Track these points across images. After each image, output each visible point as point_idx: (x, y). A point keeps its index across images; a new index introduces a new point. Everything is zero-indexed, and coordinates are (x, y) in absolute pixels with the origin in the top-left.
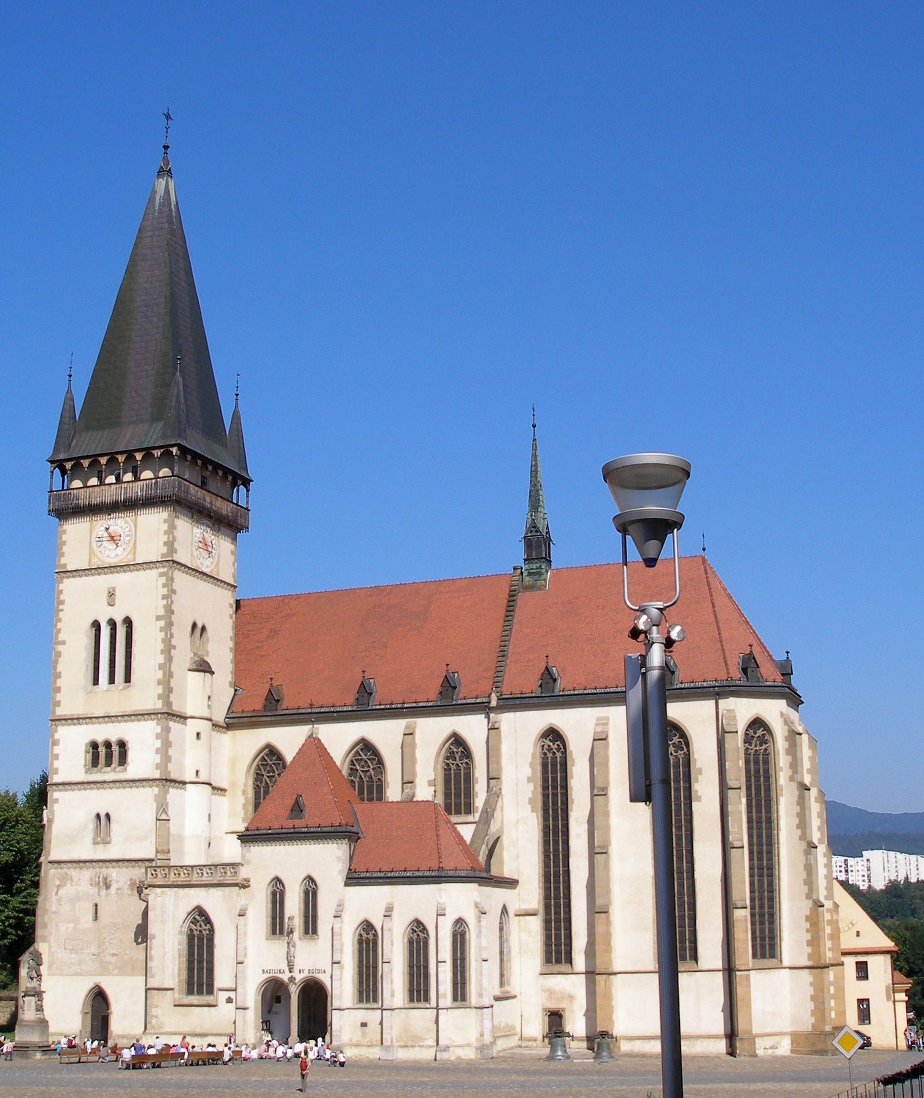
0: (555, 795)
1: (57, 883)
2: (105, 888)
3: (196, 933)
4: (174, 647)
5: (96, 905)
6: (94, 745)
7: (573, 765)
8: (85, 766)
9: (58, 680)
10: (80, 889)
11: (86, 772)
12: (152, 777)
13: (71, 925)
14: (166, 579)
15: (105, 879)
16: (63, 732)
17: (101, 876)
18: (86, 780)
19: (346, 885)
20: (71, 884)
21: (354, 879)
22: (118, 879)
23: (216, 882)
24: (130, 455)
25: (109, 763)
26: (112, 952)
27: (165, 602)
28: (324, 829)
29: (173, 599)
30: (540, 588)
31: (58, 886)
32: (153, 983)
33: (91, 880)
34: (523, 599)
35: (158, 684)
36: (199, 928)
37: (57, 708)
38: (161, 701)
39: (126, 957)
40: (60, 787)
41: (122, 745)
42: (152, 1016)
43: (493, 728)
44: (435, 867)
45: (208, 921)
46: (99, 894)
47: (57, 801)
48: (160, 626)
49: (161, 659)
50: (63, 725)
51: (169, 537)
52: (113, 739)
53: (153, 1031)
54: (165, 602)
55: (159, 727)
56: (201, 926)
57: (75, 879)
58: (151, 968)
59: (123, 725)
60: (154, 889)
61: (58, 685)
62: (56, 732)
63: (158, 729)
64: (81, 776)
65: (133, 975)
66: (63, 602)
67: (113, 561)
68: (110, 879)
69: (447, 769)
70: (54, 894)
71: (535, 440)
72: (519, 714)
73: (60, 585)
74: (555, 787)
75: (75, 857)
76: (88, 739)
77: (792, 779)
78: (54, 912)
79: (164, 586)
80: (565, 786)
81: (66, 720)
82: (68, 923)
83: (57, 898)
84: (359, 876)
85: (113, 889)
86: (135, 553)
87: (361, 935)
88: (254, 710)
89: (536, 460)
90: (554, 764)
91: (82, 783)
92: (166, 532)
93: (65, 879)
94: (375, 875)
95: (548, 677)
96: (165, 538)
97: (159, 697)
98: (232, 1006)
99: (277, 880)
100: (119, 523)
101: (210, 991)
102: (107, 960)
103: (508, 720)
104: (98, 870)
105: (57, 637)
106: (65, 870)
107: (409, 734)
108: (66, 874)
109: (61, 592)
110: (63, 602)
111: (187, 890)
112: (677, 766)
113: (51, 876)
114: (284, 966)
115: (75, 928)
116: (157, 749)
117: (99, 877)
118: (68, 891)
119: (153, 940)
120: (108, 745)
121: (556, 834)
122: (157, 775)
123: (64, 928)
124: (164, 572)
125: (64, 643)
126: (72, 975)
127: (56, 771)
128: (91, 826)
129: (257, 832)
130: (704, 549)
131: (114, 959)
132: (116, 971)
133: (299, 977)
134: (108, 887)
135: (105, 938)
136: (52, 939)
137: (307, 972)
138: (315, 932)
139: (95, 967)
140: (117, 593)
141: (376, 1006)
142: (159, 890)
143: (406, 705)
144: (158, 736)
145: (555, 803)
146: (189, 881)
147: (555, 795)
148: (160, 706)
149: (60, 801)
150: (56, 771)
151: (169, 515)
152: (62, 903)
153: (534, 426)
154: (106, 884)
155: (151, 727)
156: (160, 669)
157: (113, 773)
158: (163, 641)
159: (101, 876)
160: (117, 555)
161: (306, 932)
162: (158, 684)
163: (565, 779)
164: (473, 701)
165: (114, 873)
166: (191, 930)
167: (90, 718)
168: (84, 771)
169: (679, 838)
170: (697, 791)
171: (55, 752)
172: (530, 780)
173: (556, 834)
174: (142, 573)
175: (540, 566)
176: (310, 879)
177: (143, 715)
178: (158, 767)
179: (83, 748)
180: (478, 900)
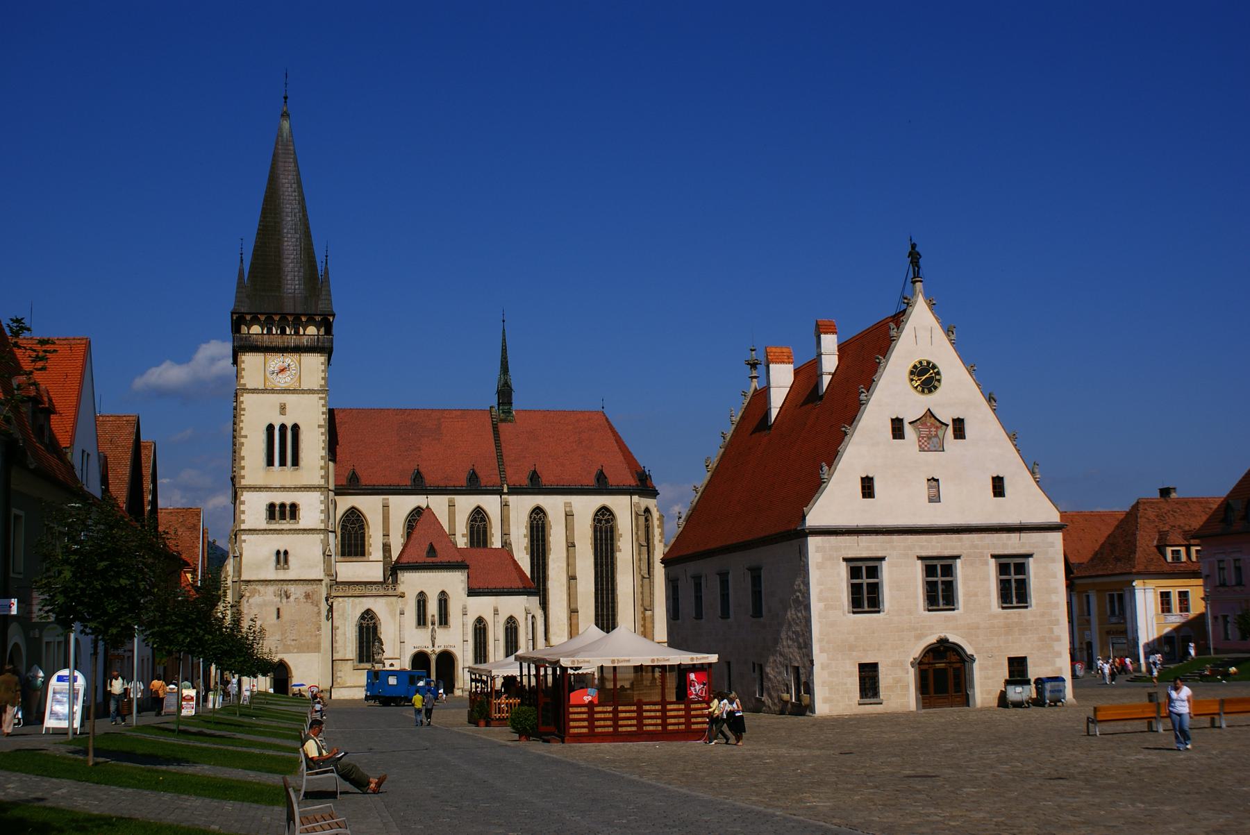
0: (538, 545)
3: (365, 625)
5: (278, 609)
6: (271, 507)
7: (551, 528)
8: (266, 519)
10: (266, 599)
11: (267, 523)
12: (318, 528)
18: (267, 528)
19: (468, 596)
21: (472, 592)
22: (296, 592)
23: (382, 594)
24: (297, 318)
25: (283, 517)
26: (294, 638)
30: (510, 421)
32: (336, 657)
33: (275, 592)
34: (503, 427)
35: (321, 469)
37: (242, 480)
38: (323, 480)
39: (303, 641)
40: (247, 532)
41: (294, 507)
42: (337, 677)
43: (505, 505)
44: (521, 586)
47: (245, 541)
50: (248, 491)
51: (325, 375)
52: (288, 502)
53: (338, 686)
54: (324, 416)
55: (323, 496)
56: (368, 621)
58: (336, 647)
60: (337, 599)
61: (242, 465)
62: (242, 495)
63: (322, 498)
65: (308, 652)
66: (244, 410)
67: (284, 386)
69: (472, 527)
71: (504, 330)
72: (519, 496)
73: (241, 398)
74: (538, 541)
75: (262, 578)
76: (268, 502)
77: (660, 541)
78: (246, 614)
79: (323, 406)
80: (544, 540)
85: (292, 599)
86: (300, 383)
87: (476, 625)
88: (342, 485)
89: (505, 343)
90: (538, 527)
93: (253, 594)
95: (534, 476)
96: (323, 375)
99: (422, 594)
100: (289, 359)
103: (512, 499)
104: (279, 586)
105: (240, 433)
106: (254, 586)
107: (452, 505)
108: (255, 589)
109: (242, 402)
110: (244, 410)
111: (360, 599)
112: (606, 532)
120: (283, 506)
121: (538, 568)
122: (322, 526)
125: (246, 437)
127: (243, 522)
128: (274, 558)
130: (603, 408)
131: (293, 643)
133: (438, 650)
134: (288, 597)
140: (287, 407)
142: (340, 599)
143: (448, 488)
144: (322, 502)
145: (538, 550)
147: (538, 545)
148: (323, 483)
150: (243, 522)
151: (325, 359)
153: (504, 321)
154: (286, 595)
155: (317, 496)
156: (322, 459)
158: (323, 441)
160: (286, 382)
161: (441, 624)
162: (321, 469)
163: (543, 536)
164: (491, 488)
165: (292, 589)
166: (362, 624)
168: (265, 522)
169: (607, 571)
170: (619, 547)
171: (242, 509)
172: (525, 536)
173: (538, 568)
174: (306, 396)
175: (510, 409)
176: (443, 593)
178: (322, 521)
179: (265, 507)
180: (527, 605)
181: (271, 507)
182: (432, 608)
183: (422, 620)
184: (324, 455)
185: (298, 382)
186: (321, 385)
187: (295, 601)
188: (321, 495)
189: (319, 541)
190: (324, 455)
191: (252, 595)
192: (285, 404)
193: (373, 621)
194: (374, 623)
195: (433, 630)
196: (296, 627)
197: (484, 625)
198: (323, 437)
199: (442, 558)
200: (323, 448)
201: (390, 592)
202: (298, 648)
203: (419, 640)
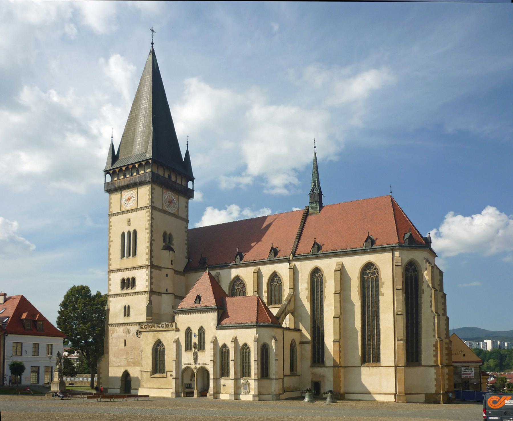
1: (111, 332)
2: (128, 333)
4: (154, 240)
5: (125, 341)
9: (110, 256)
10: (119, 334)
11: (121, 290)
13: (116, 348)
14: (149, 213)
15: (128, 330)
16: (112, 275)
17: (127, 330)
18: (121, 293)
20: (116, 333)
22: (133, 330)
26: (132, 357)
27: (149, 222)
28: (208, 308)
29: (152, 221)
31: (112, 333)
33: (123, 330)
36: (160, 348)
39: (136, 359)
41: (134, 279)
45: (163, 345)
46: (126, 336)
48: (147, 232)
49: (148, 245)
51: (150, 197)
52: (131, 277)
54: (149, 222)
55: (147, 271)
57: (118, 330)
59: (134, 271)
61: (110, 258)
64: (119, 291)
68: (130, 330)
70: (110, 336)
75: (118, 322)
76: (121, 278)
79: (148, 216)
81: (113, 271)
82: (115, 347)
83: (111, 337)
84: (222, 326)
85: (131, 334)
91: (119, 294)
92: (149, 195)
94: (229, 325)
97: (147, 259)
98: (172, 377)
101: (164, 372)
102: (130, 360)
104: (125, 326)
108: (114, 329)
113: (109, 330)
114: (192, 362)
115: (118, 348)
116: (146, 280)
117: (126, 329)
118: (115, 335)
119: (142, 353)
120: (128, 279)
123: (114, 349)
124: (148, 211)
126: (117, 366)
128: (123, 310)
129: (181, 309)
131: (132, 360)
132: (133, 365)
133: (198, 366)
134: (129, 333)
135: (129, 352)
136: (110, 353)
137: (201, 364)
138: (204, 349)
139: (125, 363)
141: (229, 378)
144: (147, 275)
146: (155, 329)
149: (112, 301)
152: (113, 339)
154: (129, 332)
156: (147, 249)
157: (131, 290)
159: (127, 330)
162: (146, 255)
167: (122, 269)
177: (140, 267)
178: (147, 287)
181: (123, 280)
182: (195, 340)
183: (188, 347)
184: (148, 246)
185: (137, 204)
186: (147, 204)
187: (133, 335)
188: (146, 270)
189: (145, 299)
190: (148, 246)
191: (113, 333)
192: (129, 219)
193: (163, 347)
194: (164, 348)
195: (196, 354)
196: (133, 351)
197: (228, 350)
198: (148, 235)
199: (203, 304)
200: (148, 241)
201: (170, 328)
202: (134, 364)
203: (187, 358)
